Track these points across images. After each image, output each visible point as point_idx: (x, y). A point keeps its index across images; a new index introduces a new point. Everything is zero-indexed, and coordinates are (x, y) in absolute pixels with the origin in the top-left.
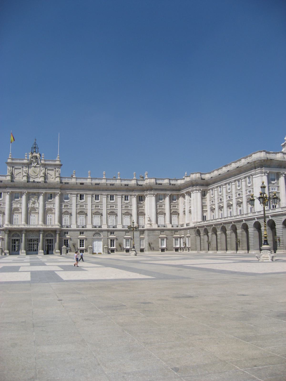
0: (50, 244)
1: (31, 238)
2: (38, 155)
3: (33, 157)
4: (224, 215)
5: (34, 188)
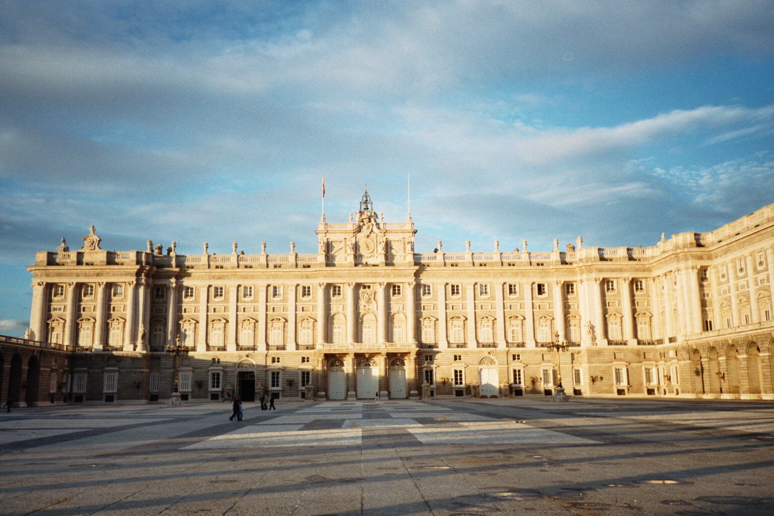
3: (363, 219)
4: (751, 318)
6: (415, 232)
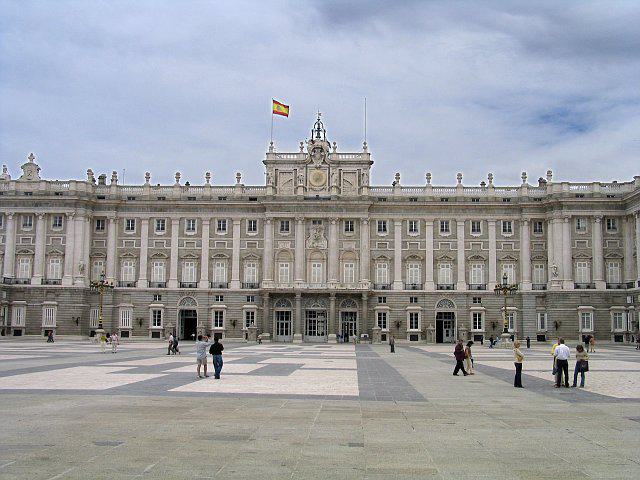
5: (317, 208)
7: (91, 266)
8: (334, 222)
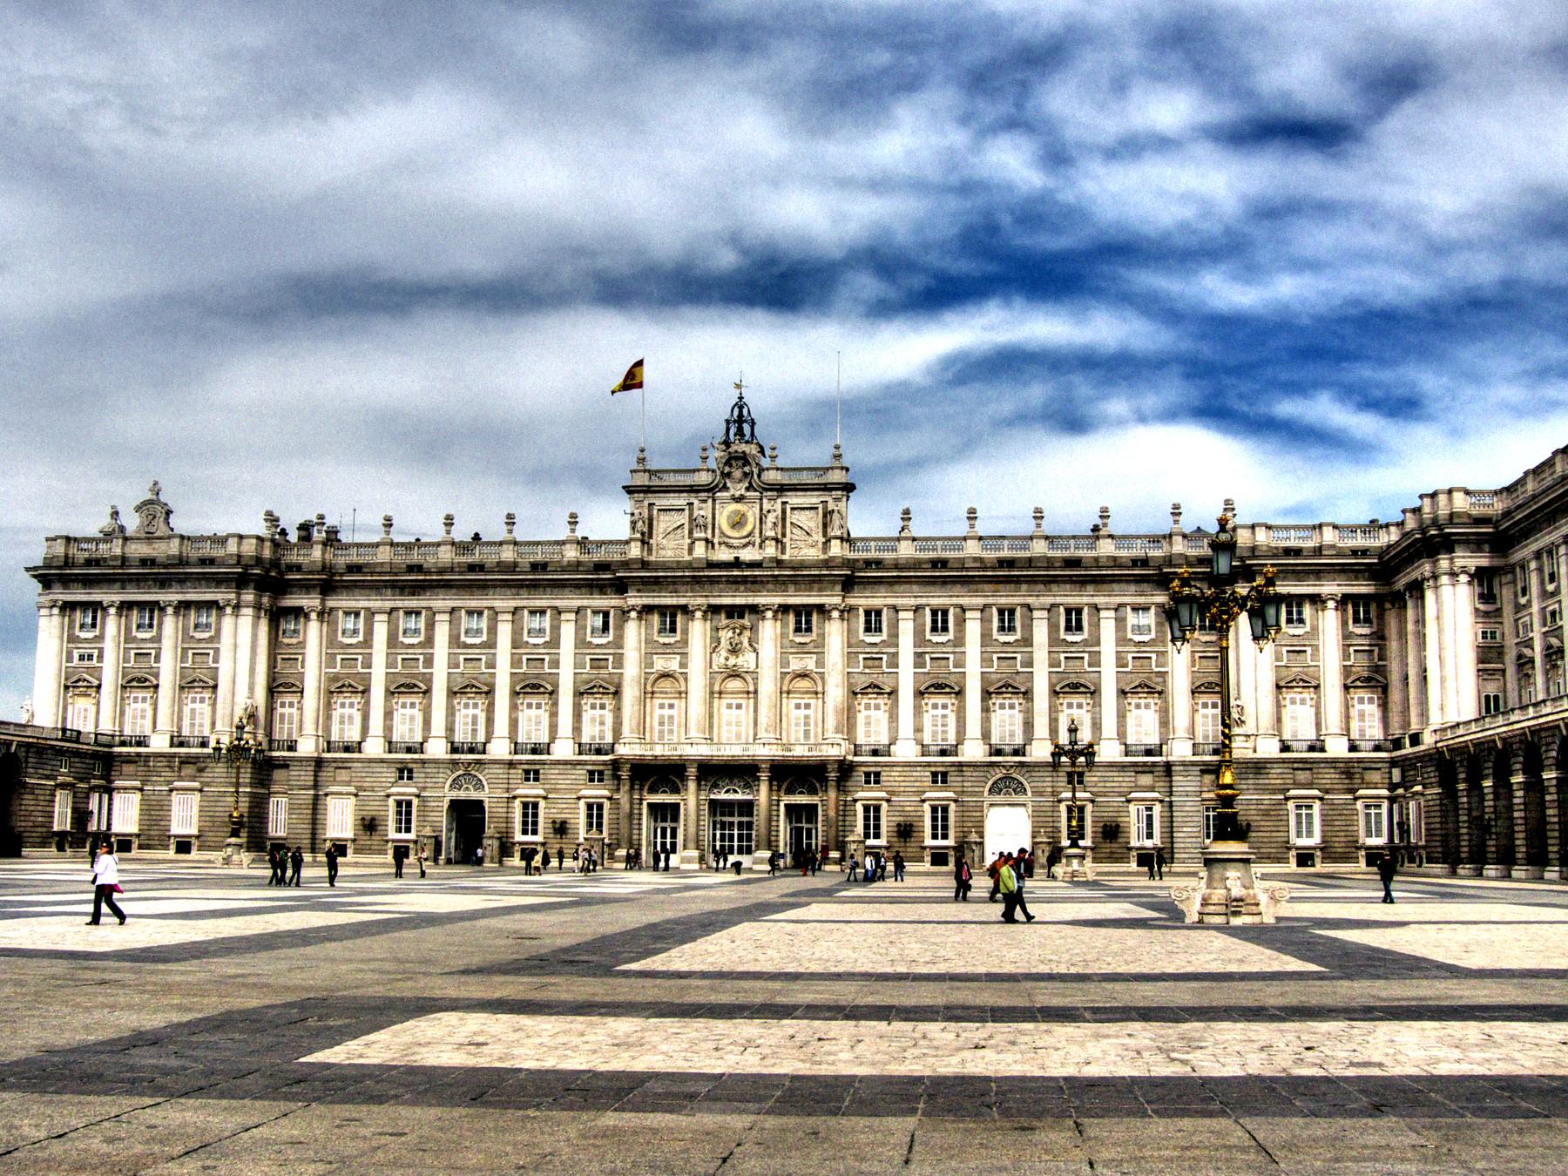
0: (809, 826)
1: (723, 796)
2: (751, 450)
6: (849, 488)
7: (270, 710)
8: (769, 614)
